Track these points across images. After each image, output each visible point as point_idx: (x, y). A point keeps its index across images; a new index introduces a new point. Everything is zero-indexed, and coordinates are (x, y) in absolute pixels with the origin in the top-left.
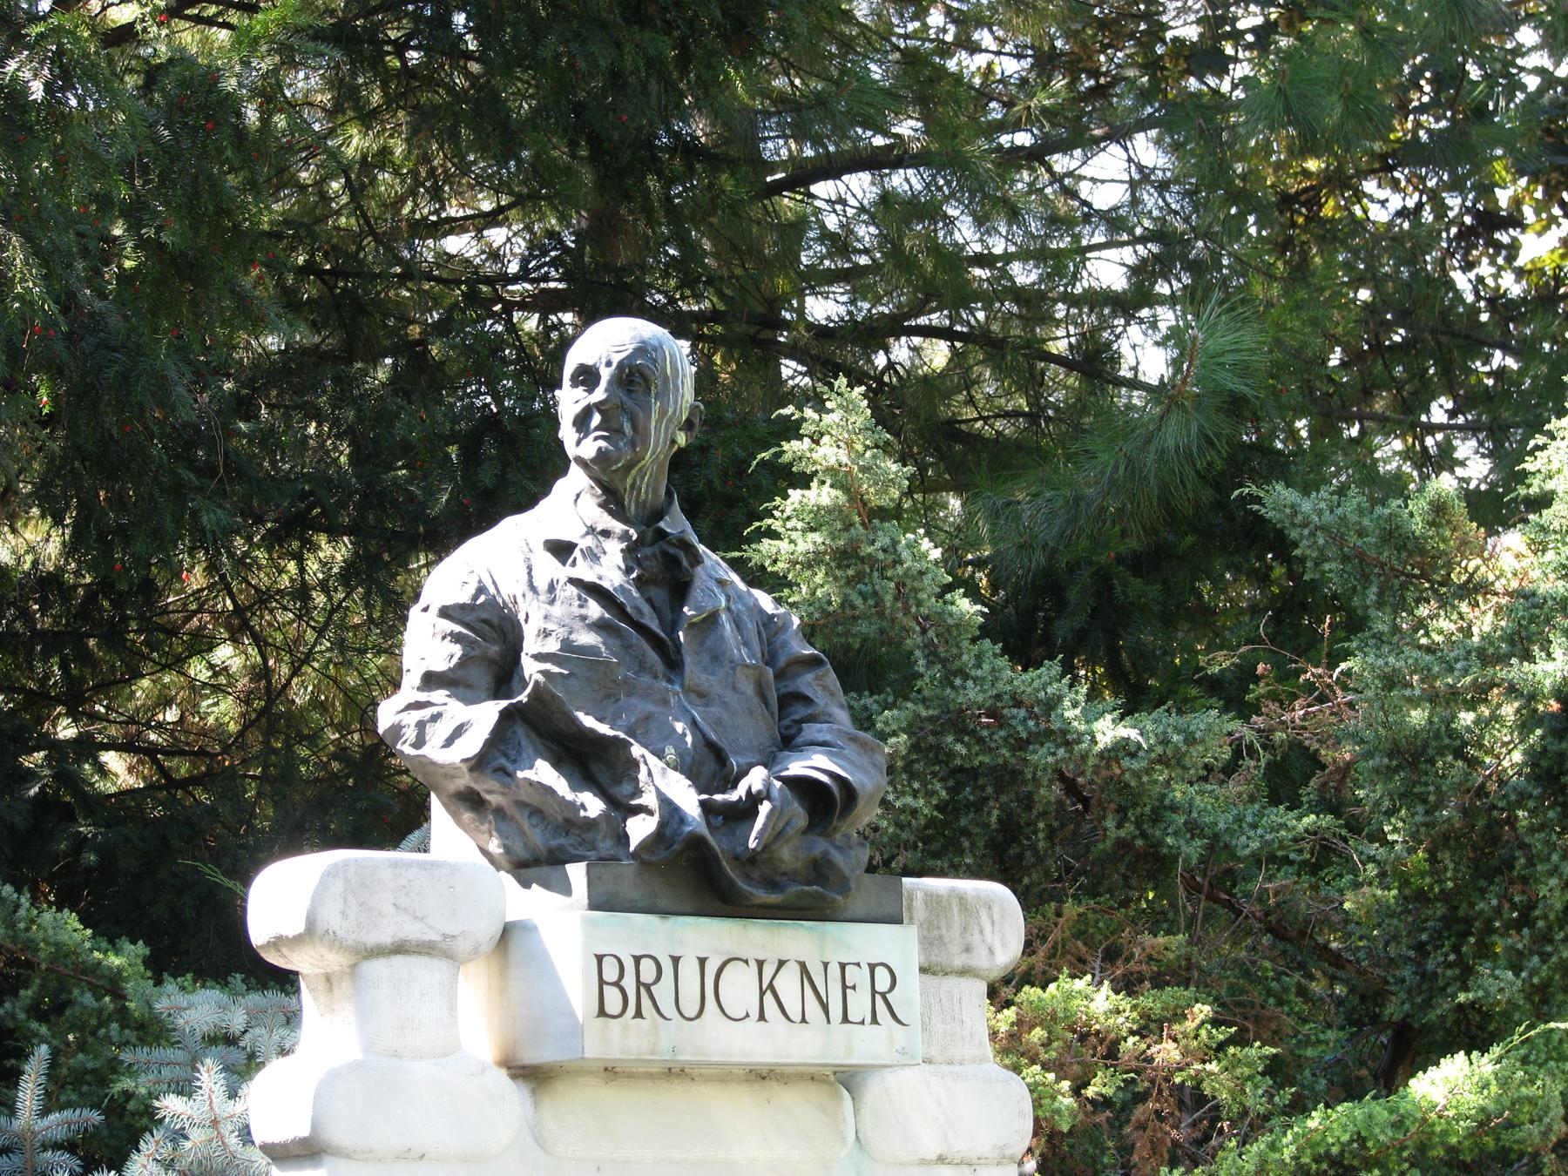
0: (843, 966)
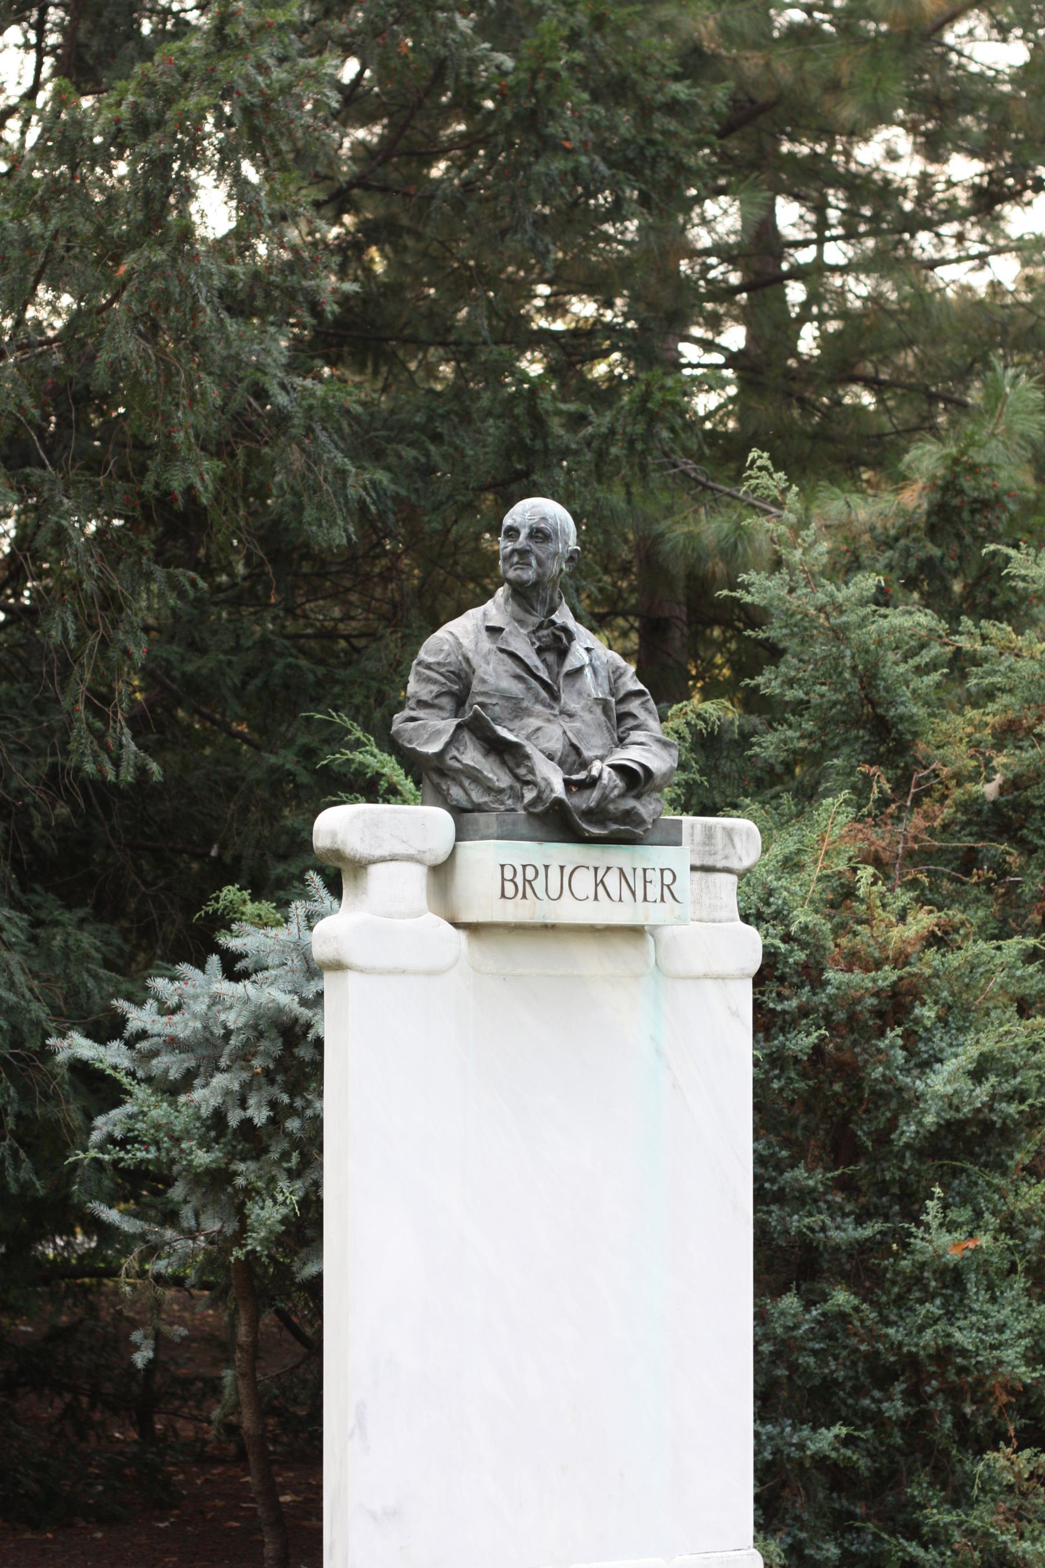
0: (645, 870)
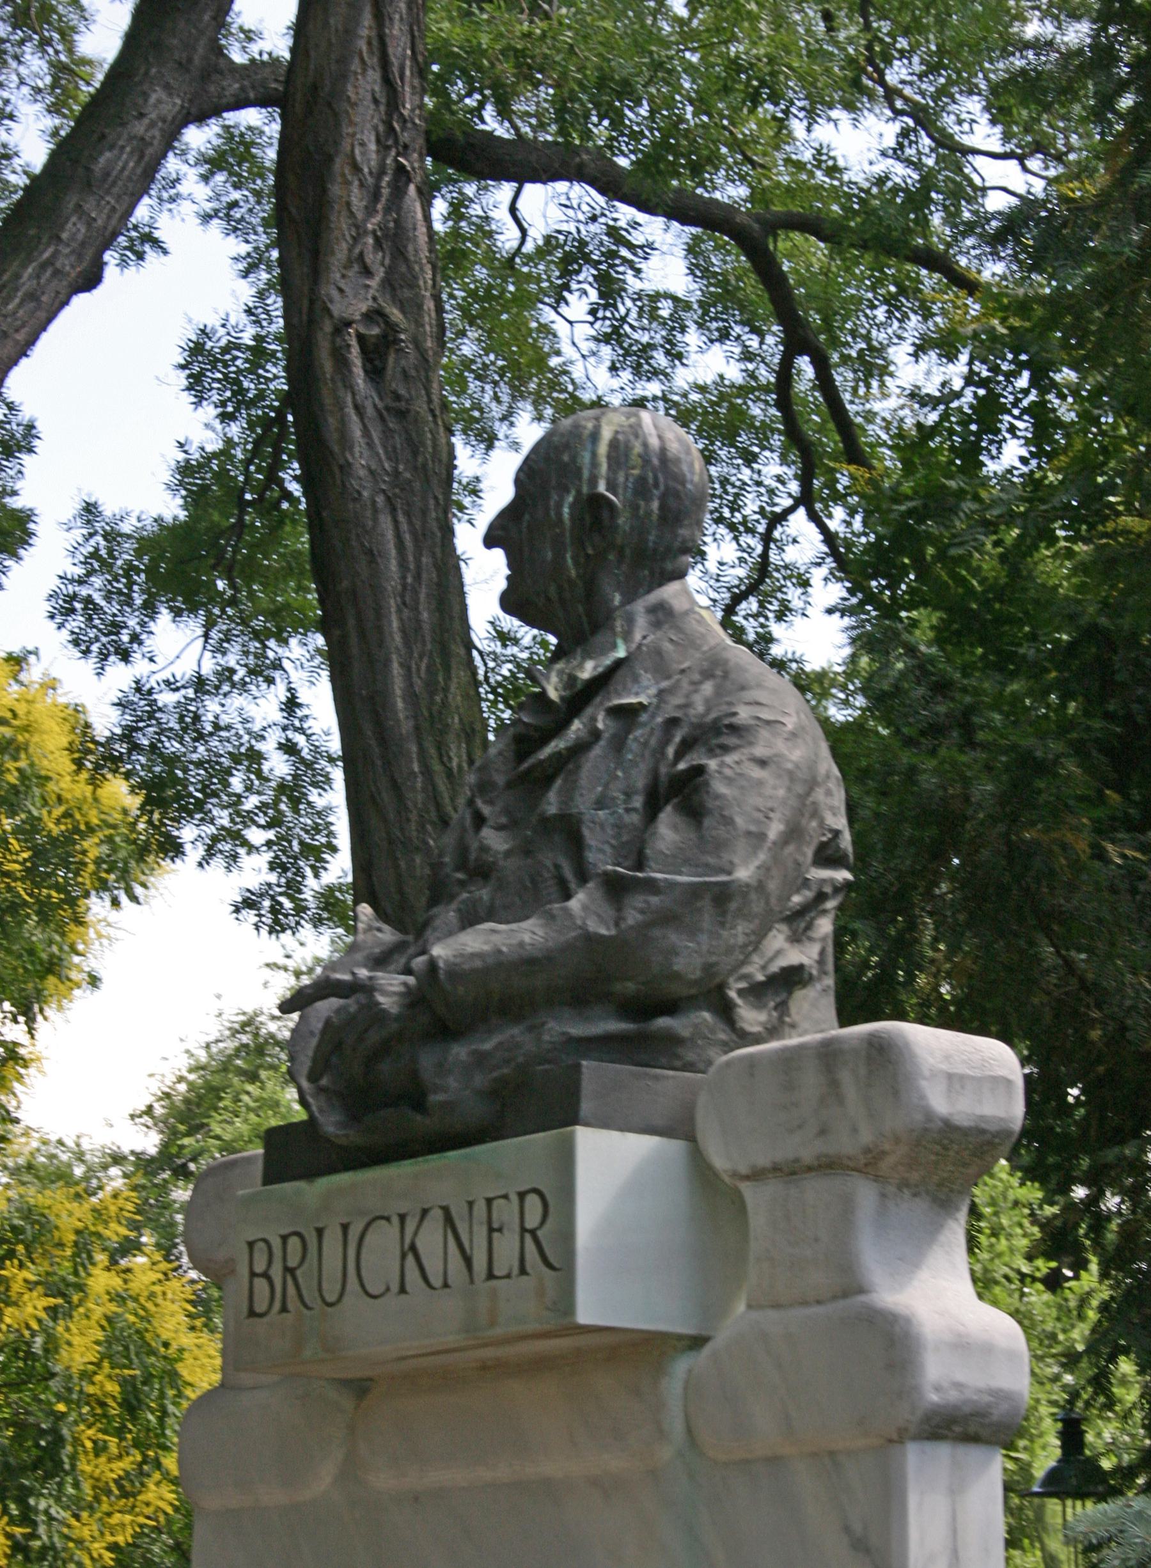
0: (489, 1201)
